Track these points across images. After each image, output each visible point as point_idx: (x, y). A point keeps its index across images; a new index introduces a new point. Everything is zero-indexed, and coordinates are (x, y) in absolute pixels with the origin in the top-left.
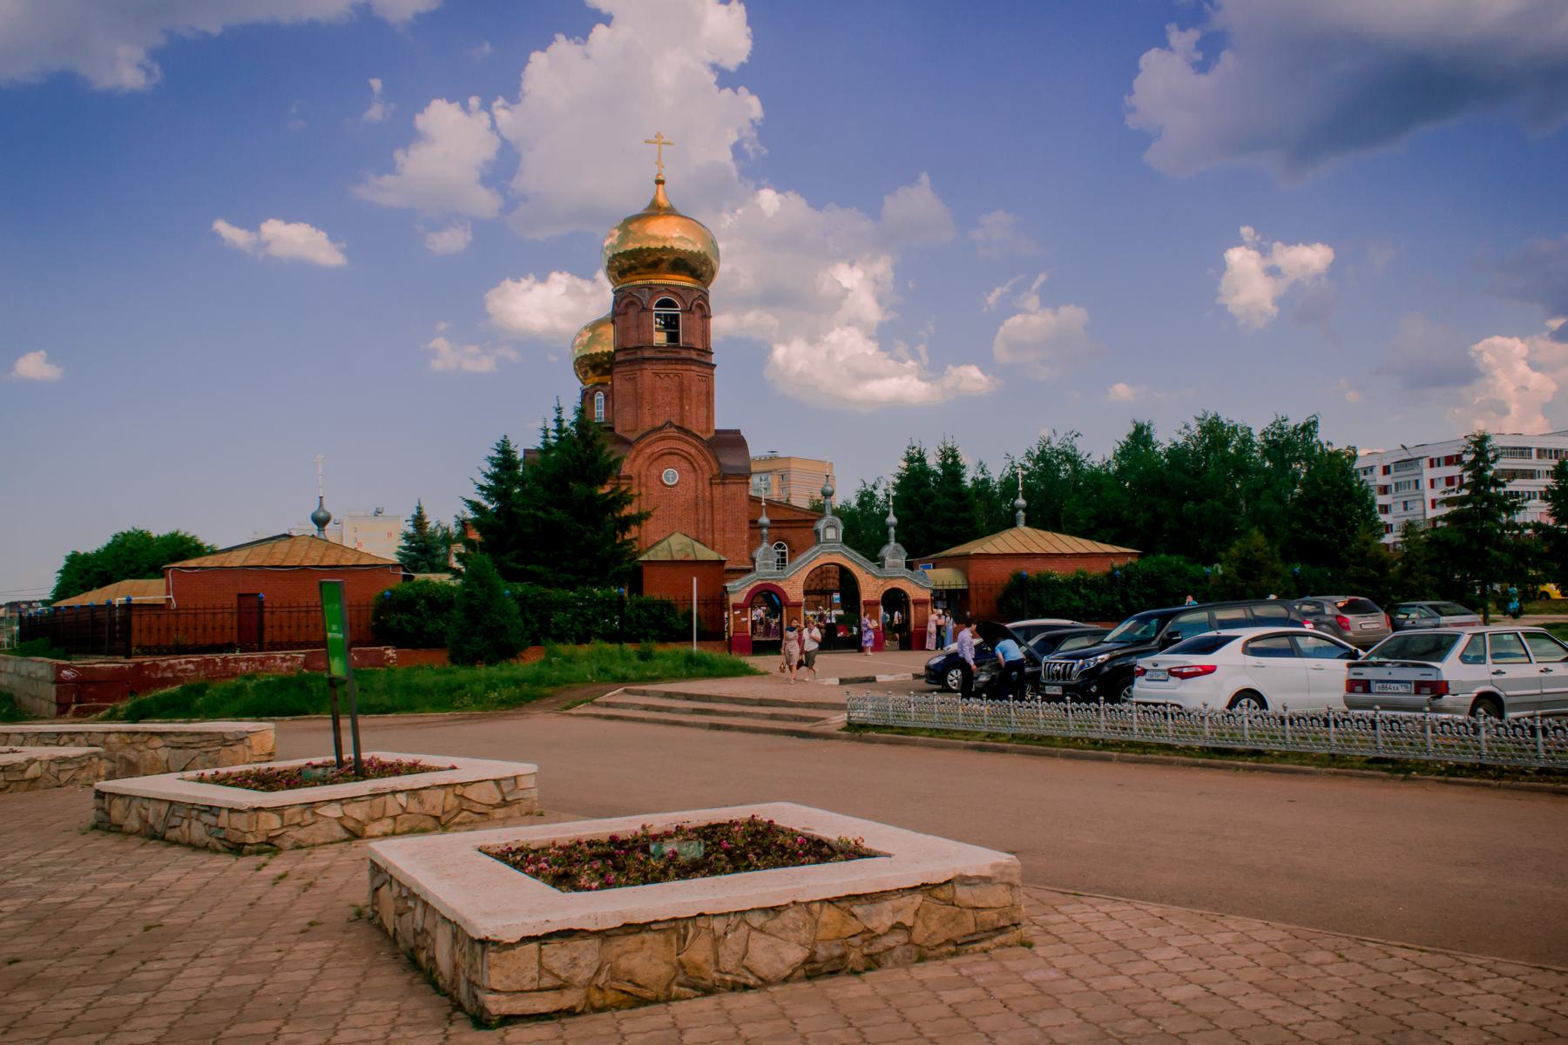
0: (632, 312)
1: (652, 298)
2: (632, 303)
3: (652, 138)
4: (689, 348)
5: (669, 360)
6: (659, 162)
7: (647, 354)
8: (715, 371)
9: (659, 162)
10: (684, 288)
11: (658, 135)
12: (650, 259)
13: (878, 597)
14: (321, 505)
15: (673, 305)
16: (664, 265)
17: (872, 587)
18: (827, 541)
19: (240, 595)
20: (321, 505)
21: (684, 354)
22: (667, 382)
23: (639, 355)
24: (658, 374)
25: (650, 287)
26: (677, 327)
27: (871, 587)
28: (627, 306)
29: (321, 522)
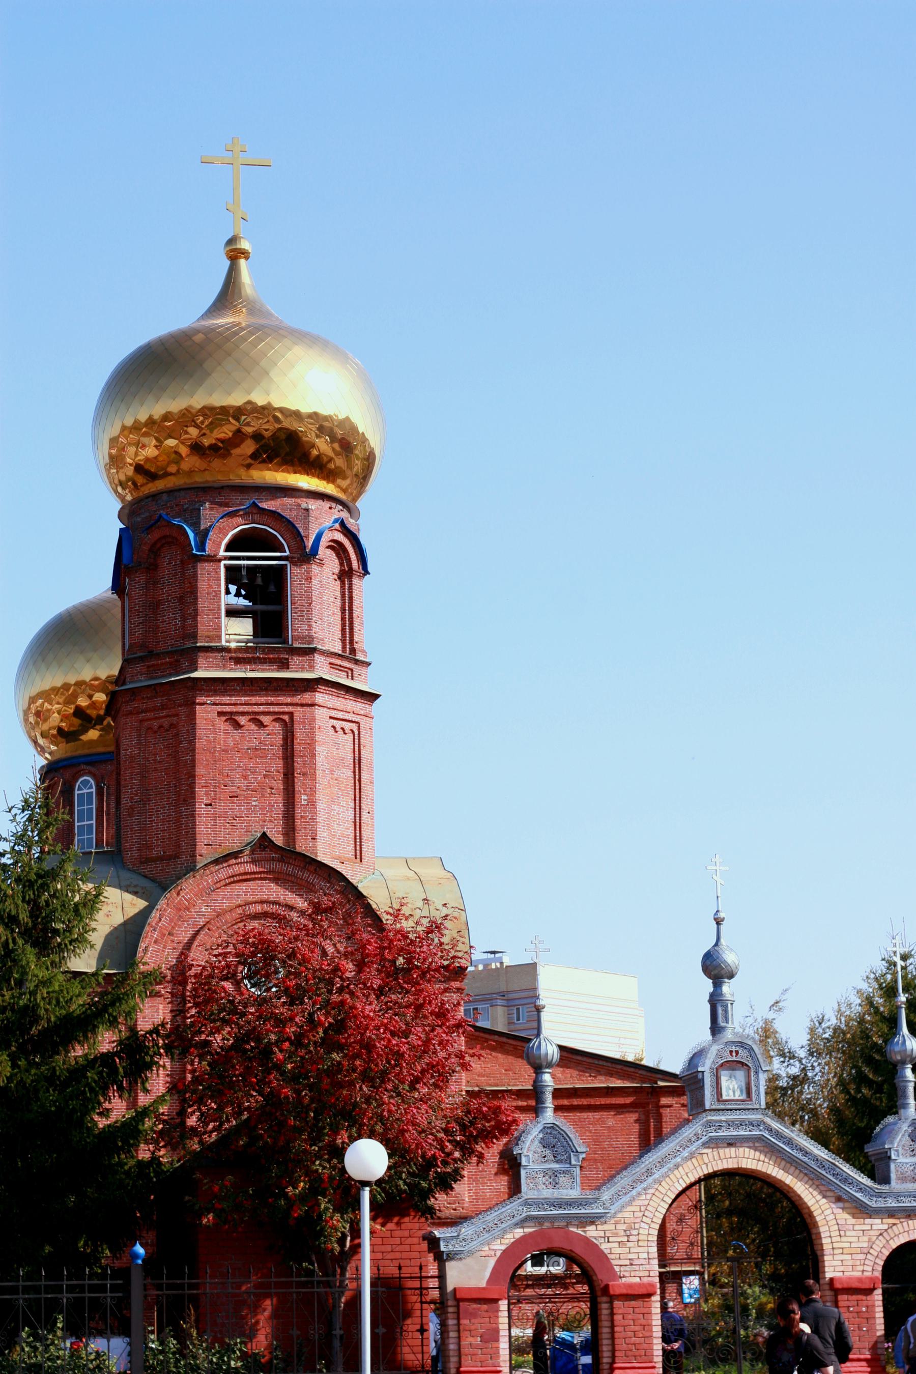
22: (251, 736)
24: (232, 719)
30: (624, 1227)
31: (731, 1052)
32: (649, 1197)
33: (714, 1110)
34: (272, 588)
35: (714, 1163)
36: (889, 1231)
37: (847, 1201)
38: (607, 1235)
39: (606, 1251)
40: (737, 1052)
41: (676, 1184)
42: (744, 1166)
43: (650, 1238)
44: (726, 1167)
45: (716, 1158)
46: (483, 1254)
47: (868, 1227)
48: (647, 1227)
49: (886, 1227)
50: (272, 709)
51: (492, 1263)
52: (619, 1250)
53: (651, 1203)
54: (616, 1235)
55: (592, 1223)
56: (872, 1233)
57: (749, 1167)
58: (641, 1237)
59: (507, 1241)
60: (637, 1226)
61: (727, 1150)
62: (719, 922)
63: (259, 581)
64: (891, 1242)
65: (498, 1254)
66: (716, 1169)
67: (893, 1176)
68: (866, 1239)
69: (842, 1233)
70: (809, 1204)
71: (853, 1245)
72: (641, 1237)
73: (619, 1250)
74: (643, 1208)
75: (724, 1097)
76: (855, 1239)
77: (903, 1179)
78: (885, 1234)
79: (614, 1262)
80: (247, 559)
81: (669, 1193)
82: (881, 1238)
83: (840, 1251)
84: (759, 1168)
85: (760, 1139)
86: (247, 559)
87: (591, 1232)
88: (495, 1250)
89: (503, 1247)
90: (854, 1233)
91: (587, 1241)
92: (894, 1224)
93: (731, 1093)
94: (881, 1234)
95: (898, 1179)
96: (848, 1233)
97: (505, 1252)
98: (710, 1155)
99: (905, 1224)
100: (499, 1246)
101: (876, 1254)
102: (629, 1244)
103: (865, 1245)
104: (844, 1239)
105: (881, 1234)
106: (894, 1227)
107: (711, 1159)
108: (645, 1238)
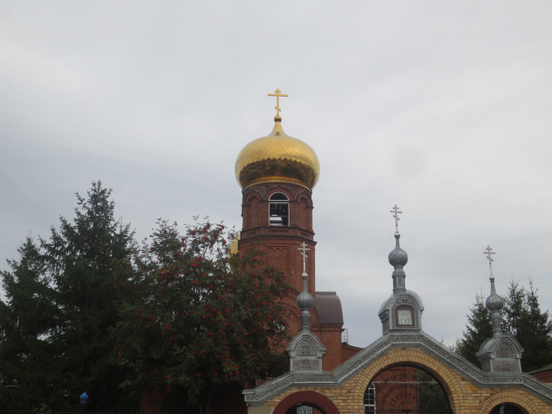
0: (254, 204)
1: (268, 192)
2: (254, 197)
3: (274, 93)
6: (277, 108)
7: (262, 232)
8: (316, 247)
9: (277, 108)
10: (292, 185)
11: (278, 92)
15: (284, 198)
17: (471, 402)
21: (291, 233)
23: (257, 233)
24: (271, 247)
25: (267, 185)
30: (345, 391)
31: (403, 300)
32: (359, 375)
33: (394, 330)
34: (284, 211)
35: (395, 358)
36: (491, 397)
37: (468, 381)
38: (336, 395)
39: (336, 404)
40: (406, 300)
41: (374, 369)
42: (411, 360)
43: (360, 398)
44: (401, 360)
45: (396, 355)
46: (268, 404)
47: (479, 395)
48: (358, 391)
49: (489, 395)
50: (283, 245)
52: (343, 404)
53: (361, 379)
54: (341, 396)
55: (328, 389)
56: (481, 398)
57: (414, 361)
58: (355, 397)
59: (282, 397)
60: (353, 391)
61: (402, 352)
62: (397, 237)
63: (280, 209)
64: (492, 403)
65: (277, 404)
66: (396, 361)
67: (492, 367)
68: (478, 401)
69: (465, 398)
70: (447, 381)
71: (471, 405)
72: (355, 397)
73: (343, 404)
74: (356, 382)
75: (400, 324)
76: (472, 401)
78: (489, 399)
79: (340, 411)
80: (277, 202)
81: (370, 374)
82: (486, 401)
83: (464, 408)
84: (419, 362)
85: (419, 346)
86: (277, 202)
87: (328, 394)
88: (275, 402)
89: (279, 401)
90: (471, 398)
91: (326, 398)
92: (493, 394)
93: (404, 321)
94: (486, 399)
95: (494, 369)
96: (469, 398)
97: (280, 404)
98: (393, 354)
99: (500, 394)
100: (277, 400)
101: (484, 409)
102: (348, 401)
103: (478, 405)
104: (466, 401)
105: (486, 399)
106: (494, 396)
107: (393, 356)
108: (357, 397)
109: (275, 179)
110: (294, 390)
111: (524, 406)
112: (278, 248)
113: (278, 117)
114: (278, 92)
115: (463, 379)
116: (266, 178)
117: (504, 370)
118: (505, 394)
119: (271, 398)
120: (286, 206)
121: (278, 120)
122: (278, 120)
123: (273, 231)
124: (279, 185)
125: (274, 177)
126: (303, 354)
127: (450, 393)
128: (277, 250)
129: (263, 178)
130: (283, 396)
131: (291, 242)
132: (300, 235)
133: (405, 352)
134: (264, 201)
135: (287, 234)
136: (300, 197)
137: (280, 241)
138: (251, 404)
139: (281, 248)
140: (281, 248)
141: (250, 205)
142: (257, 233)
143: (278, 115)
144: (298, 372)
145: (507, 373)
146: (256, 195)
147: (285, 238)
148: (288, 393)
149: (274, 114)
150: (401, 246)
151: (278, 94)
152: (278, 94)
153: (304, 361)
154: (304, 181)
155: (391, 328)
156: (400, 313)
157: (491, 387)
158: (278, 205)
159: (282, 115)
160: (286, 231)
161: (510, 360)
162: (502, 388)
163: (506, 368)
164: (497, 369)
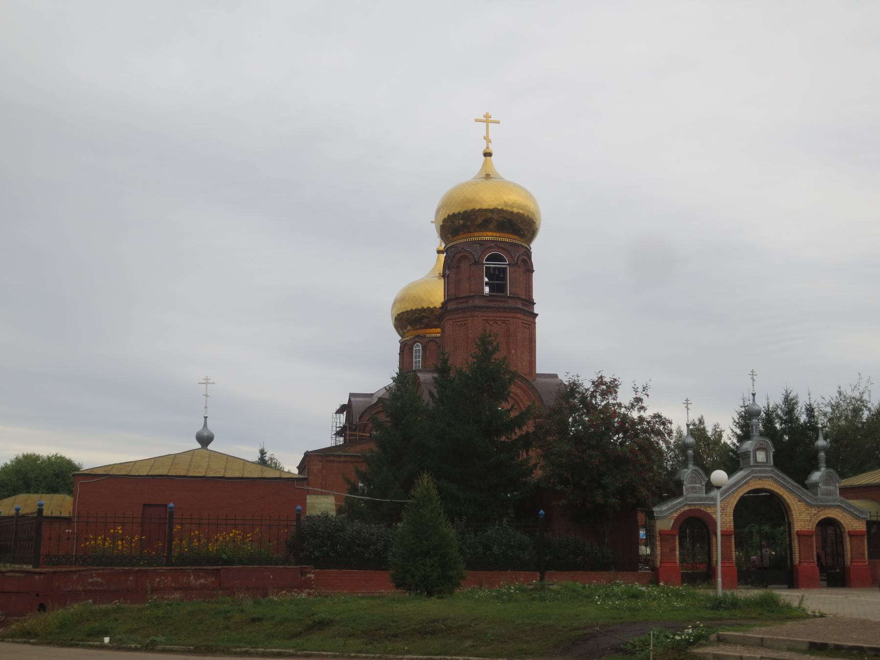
0: (464, 266)
1: (483, 253)
2: (465, 257)
3: (482, 118)
4: (515, 298)
5: (498, 309)
6: (487, 139)
7: (477, 302)
8: (537, 320)
9: (487, 139)
11: (487, 116)
12: (480, 220)
13: (811, 527)
14: (205, 425)
15: (501, 259)
16: (492, 226)
17: (804, 516)
18: (757, 464)
19: (145, 505)
20: (205, 425)
21: (511, 304)
23: (470, 303)
24: (487, 321)
25: (481, 243)
26: (504, 279)
27: (803, 517)
28: (460, 260)
29: (205, 440)
51: (672, 521)
77: (823, 494)
80: (493, 265)
85: (771, 477)
86: (493, 265)
87: (709, 511)
97: (677, 518)
100: (675, 515)
109: (488, 236)
110: (687, 508)
111: (839, 519)
112: (496, 322)
113: (488, 151)
114: (487, 116)
115: (800, 501)
116: (480, 234)
117: (827, 495)
118: (827, 511)
119: (671, 513)
120: (504, 269)
121: (487, 154)
122: (487, 154)
123: (490, 301)
124: (498, 244)
125: (485, 234)
126: (692, 482)
127: (791, 510)
128: (495, 325)
129: (476, 234)
130: (679, 512)
131: (511, 315)
132: (520, 306)
133: (761, 482)
134: (478, 263)
135: (506, 305)
136: (521, 258)
137: (499, 314)
138: (658, 518)
139: (500, 323)
140: (500, 323)
141: (458, 267)
142: (470, 303)
143: (488, 148)
144: (690, 495)
145: (830, 497)
146: (467, 254)
147: (505, 310)
148: (683, 510)
149: (482, 148)
150: (757, 401)
151: (487, 120)
152: (487, 120)
153: (693, 488)
154: (522, 236)
155: (752, 464)
156: (758, 453)
157: (818, 506)
158: (494, 268)
159: (492, 148)
160: (505, 301)
161: (831, 488)
162: (826, 507)
163: (829, 493)
164: (823, 494)
